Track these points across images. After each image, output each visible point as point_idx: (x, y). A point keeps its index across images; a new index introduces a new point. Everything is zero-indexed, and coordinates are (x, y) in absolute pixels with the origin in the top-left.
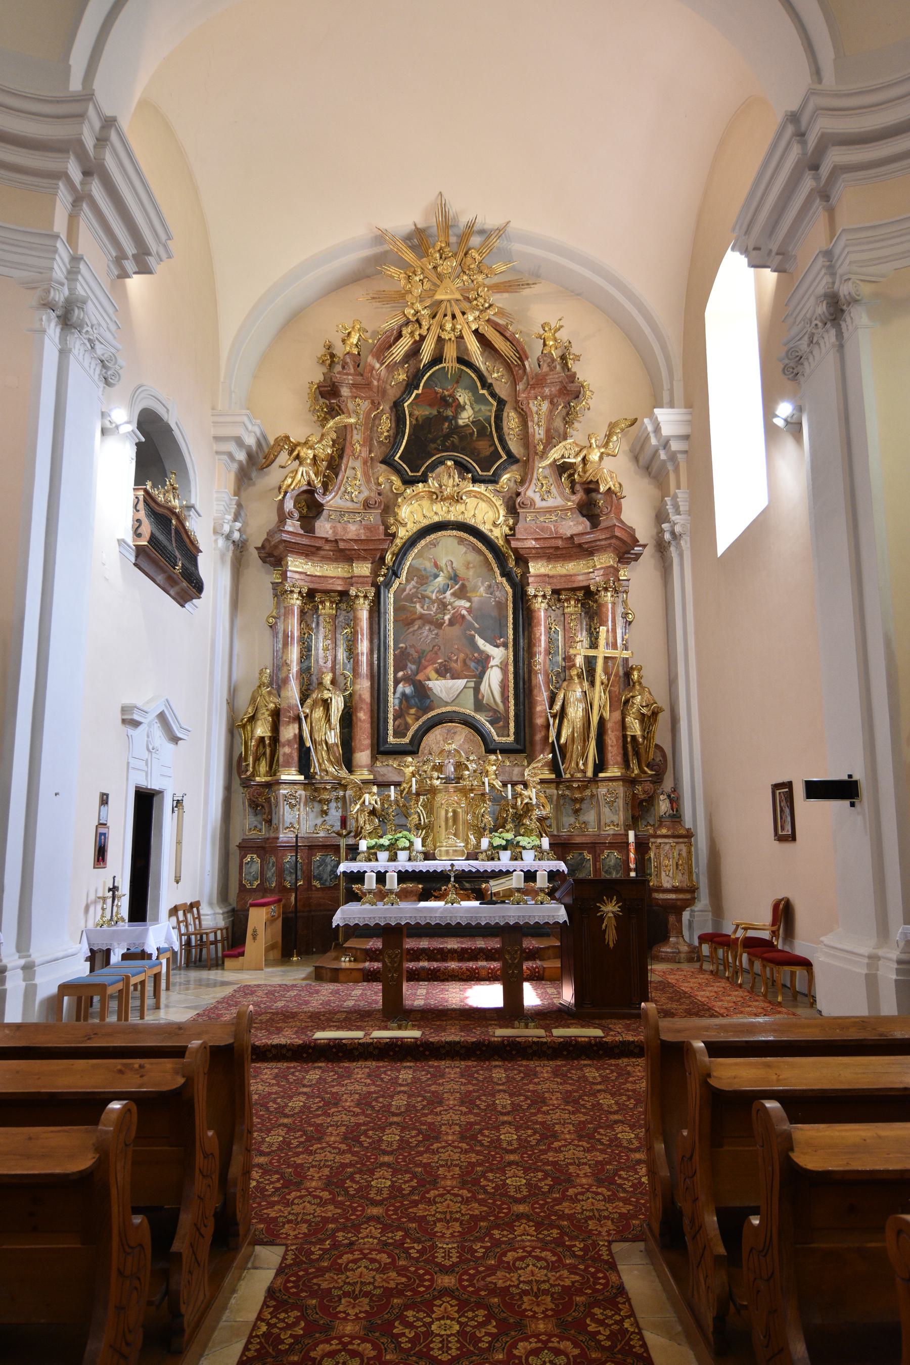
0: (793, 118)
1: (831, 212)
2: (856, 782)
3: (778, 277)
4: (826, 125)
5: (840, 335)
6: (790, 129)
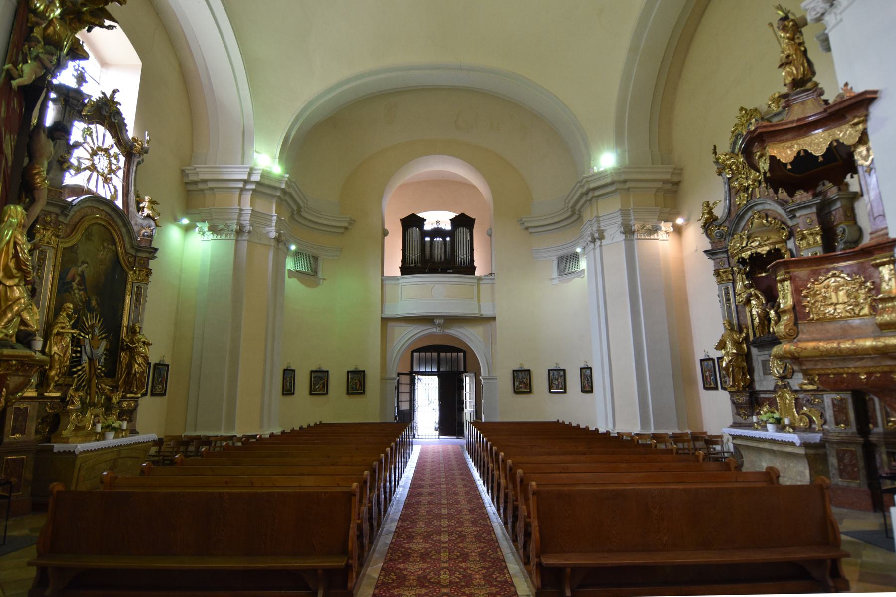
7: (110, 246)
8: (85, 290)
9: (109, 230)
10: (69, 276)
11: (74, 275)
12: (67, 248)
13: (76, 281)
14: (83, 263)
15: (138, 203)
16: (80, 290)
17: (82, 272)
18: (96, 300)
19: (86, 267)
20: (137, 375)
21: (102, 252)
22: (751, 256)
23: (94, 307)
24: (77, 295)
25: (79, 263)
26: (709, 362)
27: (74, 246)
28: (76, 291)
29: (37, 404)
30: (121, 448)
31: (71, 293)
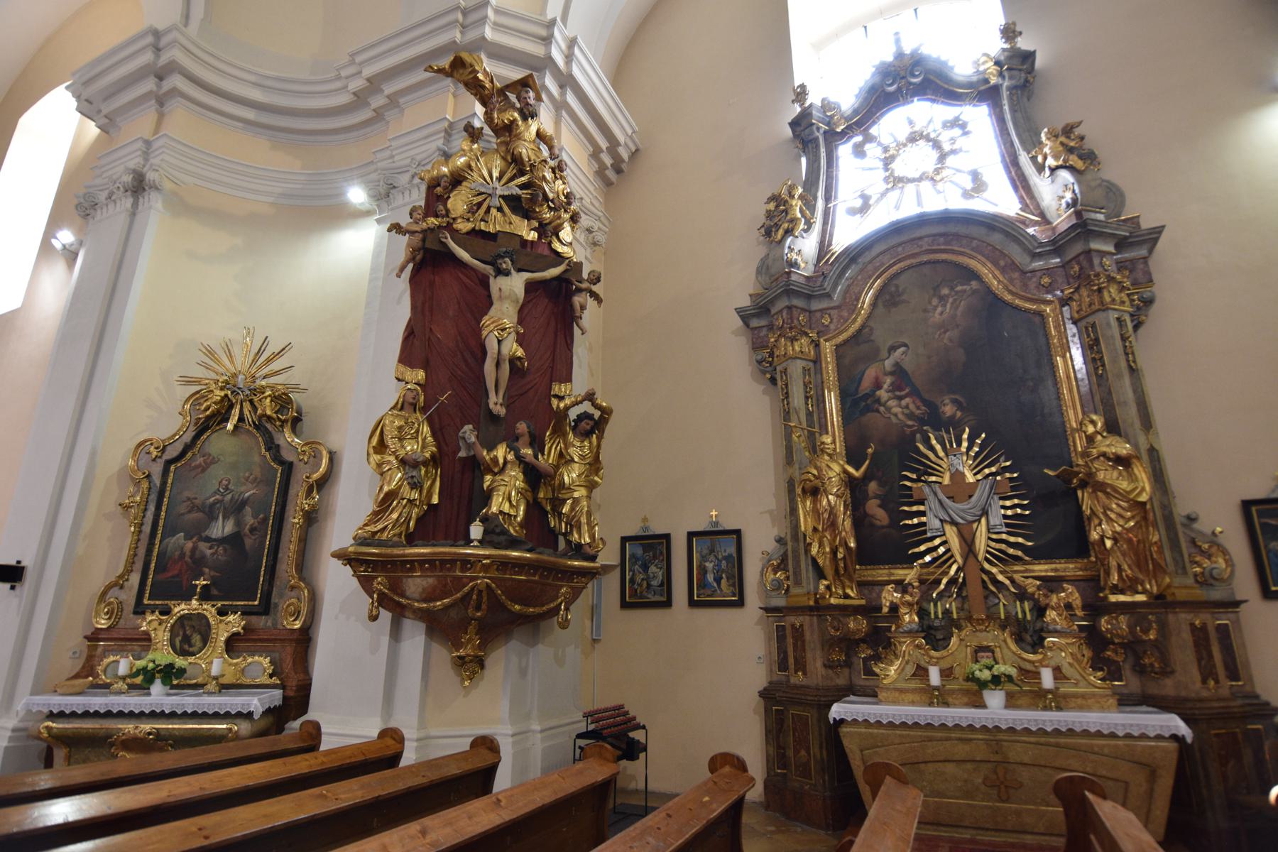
0: (157, 34)
1: (161, 116)
2: (23, 568)
3: (99, 136)
4: (177, 55)
5: (135, 205)
6: (150, 39)
7: (959, 288)
8: (915, 393)
9: (944, 261)
10: (866, 384)
11: (877, 378)
12: (846, 342)
13: (885, 386)
14: (893, 349)
15: (1034, 159)
16: (900, 398)
17: (897, 365)
18: (955, 402)
19: (904, 353)
20: (1109, 543)
21: (939, 309)
23: (954, 416)
24: (896, 410)
25: (884, 353)
27: (860, 331)
28: (892, 403)
29: (815, 618)
30: (1001, 736)
31: (878, 411)
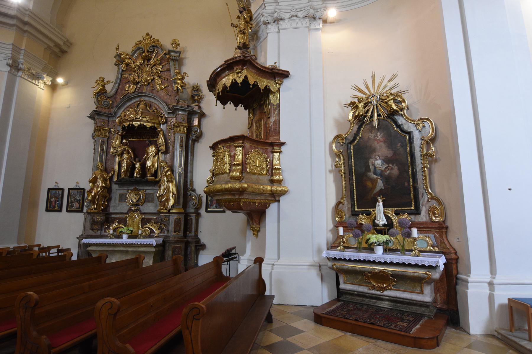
22: (129, 125)
26: (58, 191)
